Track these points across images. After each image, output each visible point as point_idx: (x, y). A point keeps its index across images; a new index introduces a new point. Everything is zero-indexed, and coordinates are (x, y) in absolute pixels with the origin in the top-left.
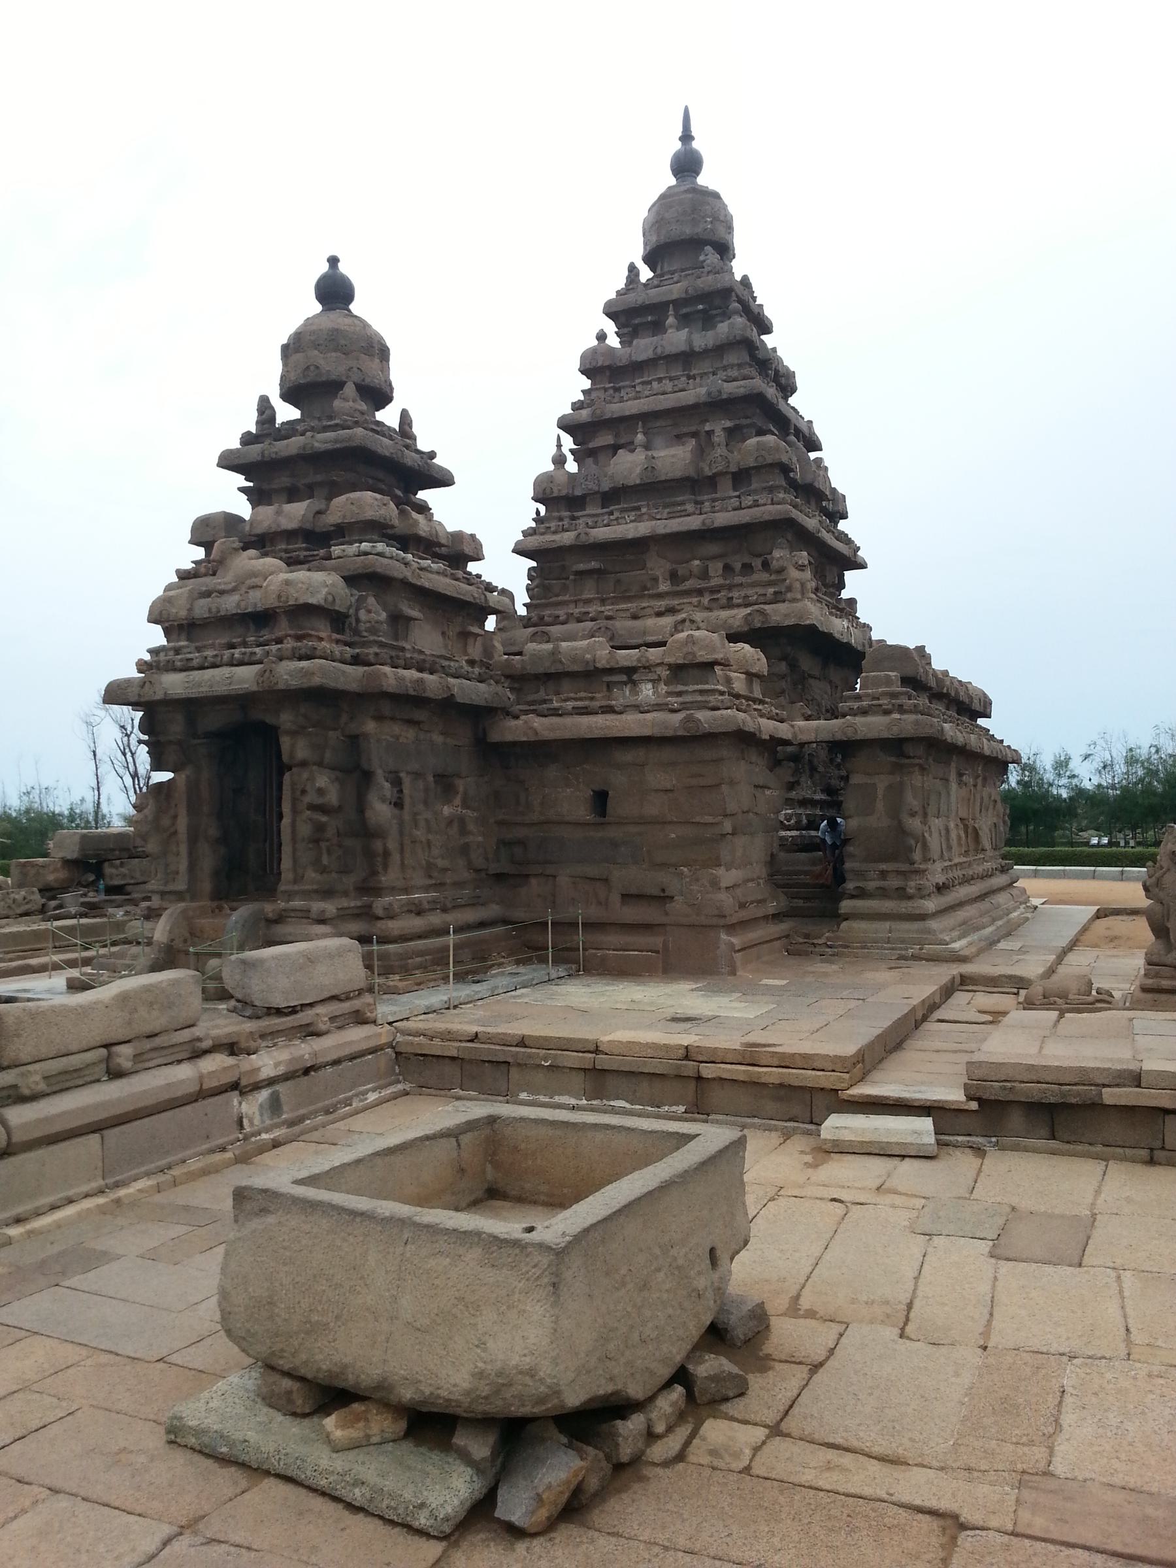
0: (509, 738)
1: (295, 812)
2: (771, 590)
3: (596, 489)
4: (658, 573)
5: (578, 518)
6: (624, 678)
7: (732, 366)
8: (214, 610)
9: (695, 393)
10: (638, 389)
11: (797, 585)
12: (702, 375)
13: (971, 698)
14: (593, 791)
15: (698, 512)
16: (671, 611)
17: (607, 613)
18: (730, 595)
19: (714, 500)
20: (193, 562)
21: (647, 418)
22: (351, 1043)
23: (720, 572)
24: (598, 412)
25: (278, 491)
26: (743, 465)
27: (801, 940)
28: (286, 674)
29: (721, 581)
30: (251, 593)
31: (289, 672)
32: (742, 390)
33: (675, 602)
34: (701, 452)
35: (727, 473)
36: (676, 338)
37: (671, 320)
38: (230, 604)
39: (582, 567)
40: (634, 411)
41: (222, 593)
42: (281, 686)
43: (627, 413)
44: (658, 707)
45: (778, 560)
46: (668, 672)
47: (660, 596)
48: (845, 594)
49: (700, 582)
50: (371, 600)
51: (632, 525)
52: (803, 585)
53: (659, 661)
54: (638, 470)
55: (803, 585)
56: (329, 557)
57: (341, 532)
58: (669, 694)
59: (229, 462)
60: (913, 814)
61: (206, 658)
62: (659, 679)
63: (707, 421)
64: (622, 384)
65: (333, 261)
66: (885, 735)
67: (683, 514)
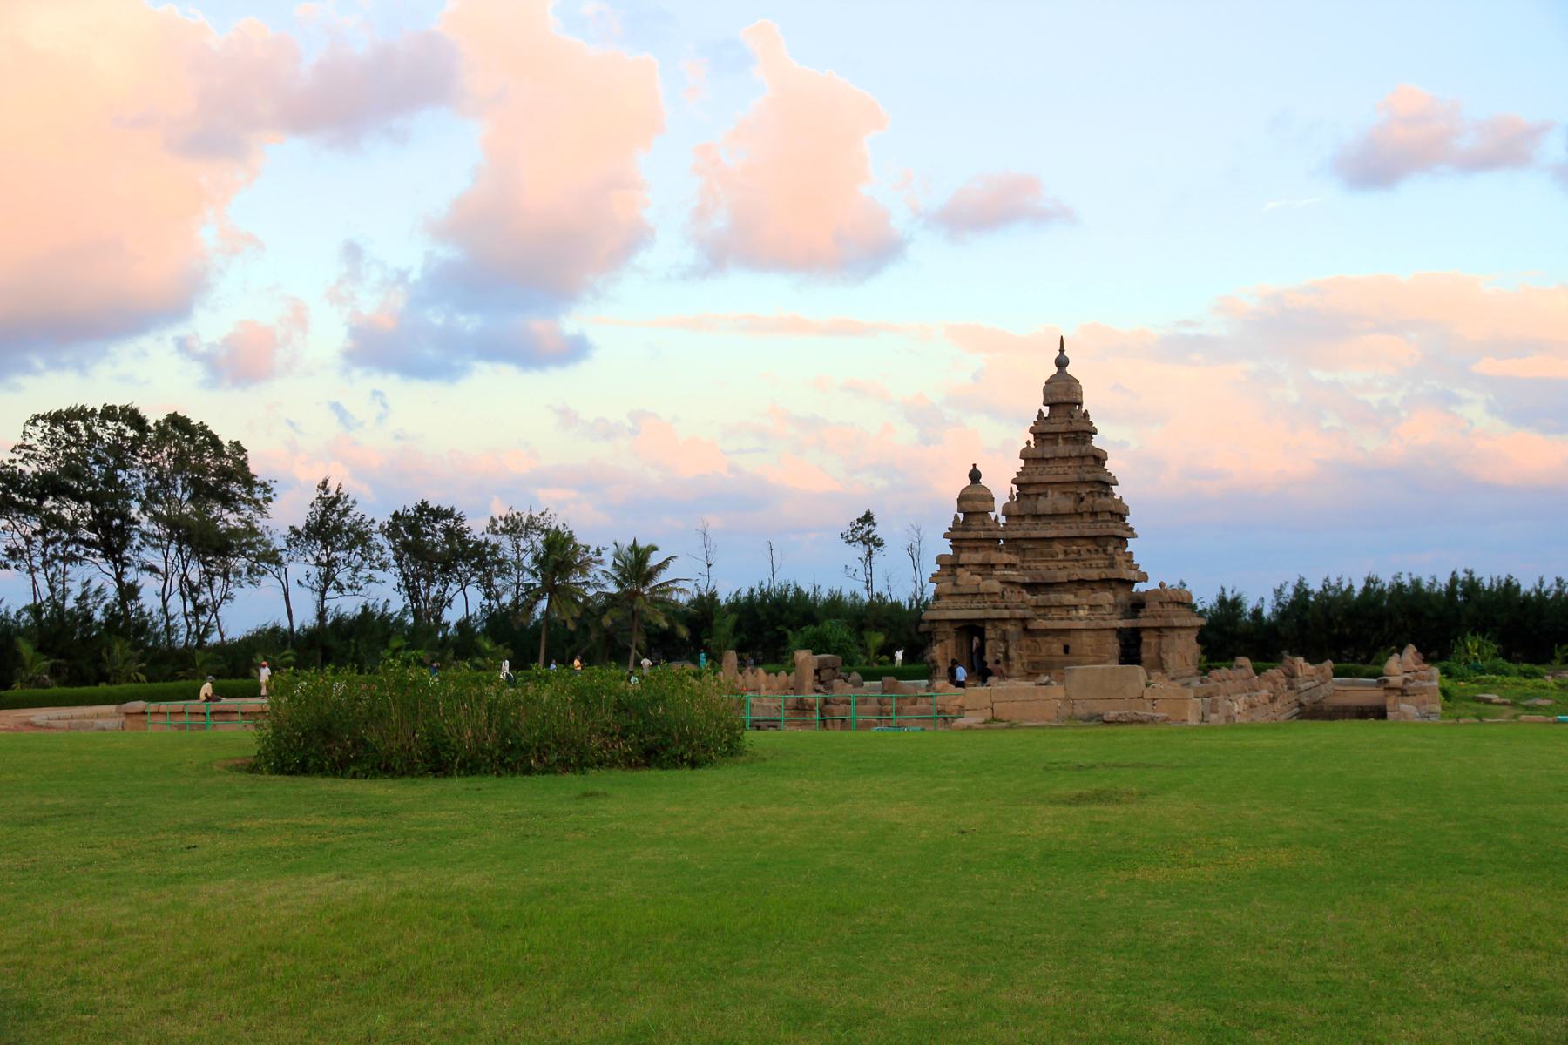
2: (1107, 562)
9: (1072, 477)
10: (1048, 469)
13: (1183, 598)
16: (1065, 567)
25: (965, 547)
31: (994, 614)
32: (1093, 479)
37: (1060, 441)
40: (1047, 481)
44: (1086, 619)
47: (1060, 561)
48: (1128, 550)
59: (946, 536)
60: (1164, 652)
65: (974, 465)
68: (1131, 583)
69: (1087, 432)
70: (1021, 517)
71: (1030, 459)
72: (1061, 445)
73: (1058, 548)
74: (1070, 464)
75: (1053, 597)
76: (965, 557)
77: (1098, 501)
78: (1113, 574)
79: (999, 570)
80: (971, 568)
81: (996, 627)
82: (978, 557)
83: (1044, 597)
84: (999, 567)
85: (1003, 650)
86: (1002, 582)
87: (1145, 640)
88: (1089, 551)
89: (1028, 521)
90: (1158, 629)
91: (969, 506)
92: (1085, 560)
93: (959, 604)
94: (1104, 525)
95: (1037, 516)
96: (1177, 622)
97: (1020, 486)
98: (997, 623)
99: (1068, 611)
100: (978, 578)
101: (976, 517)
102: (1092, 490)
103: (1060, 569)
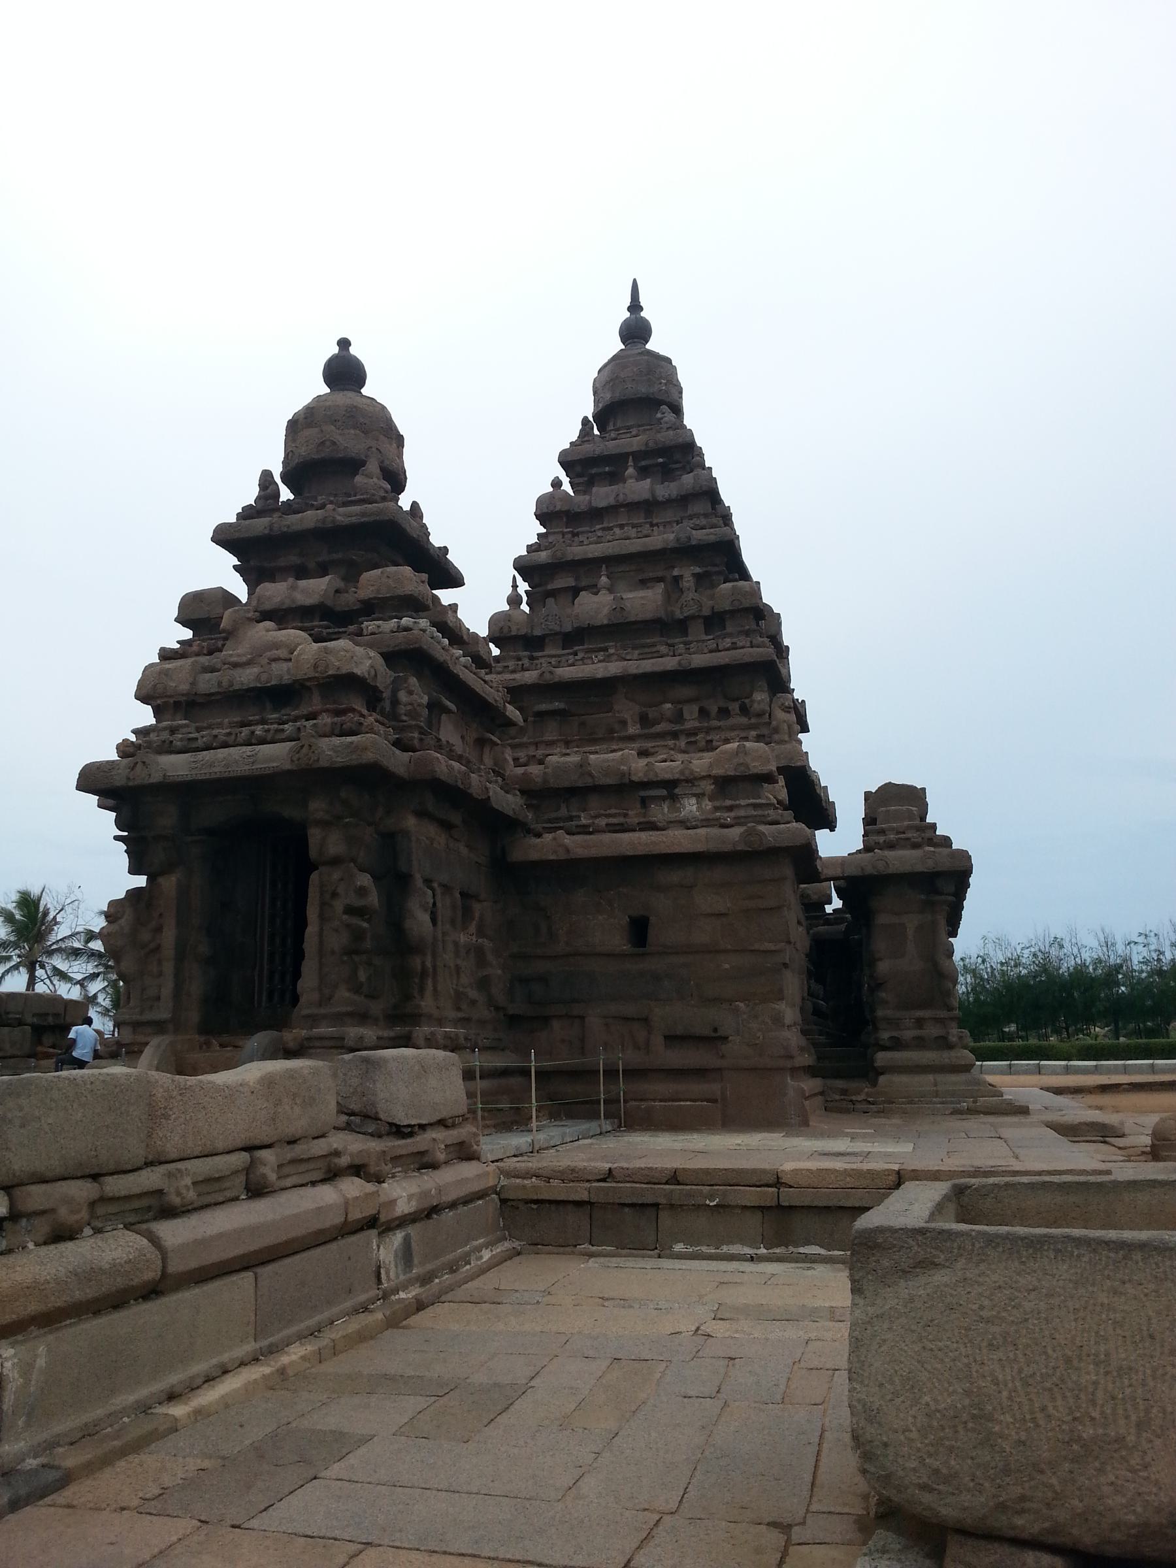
0: (534, 856)
1: (322, 918)
3: (557, 629)
4: (627, 716)
5: (537, 658)
6: (664, 792)
7: (697, 516)
8: (225, 684)
12: (665, 524)
14: (629, 917)
15: (672, 653)
18: (709, 738)
20: (178, 642)
21: (610, 561)
22: (465, 1180)
23: (696, 714)
24: (559, 554)
26: (717, 609)
27: (837, 1097)
28: (329, 750)
29: (697, 724)
30: (274, 665)
32: (712, 538)
33: (649, 745)
34: (668, 596)
35: (699, 617)
36: (637, 488)
37: (631, 471)
38: (246, 677)
39: (543, 707)
40: (596, 554)
41: (235, 665)
42: (324, 763)
43: (590, 556)
44: (707, 823)
45: (759, 702)
46: (713, 787)
47: (631, 738)
49: (673, 726)
50: (413, 680)
51: (600, 665)
52: (789, 727)
53: (704, 774)
54: (606, 611)
55: (789, 727)
56: (360, 634)
57: (370, 608)
58: (716, 809)
61: (216, 736)
62: (703, 794)
63: (673, 567)
64: (580, 529)
65: (344, 344)
66: (920, 868)
67: (655, 655)
74: (655, 521)
87: (882, 919)
94: (742, 641)
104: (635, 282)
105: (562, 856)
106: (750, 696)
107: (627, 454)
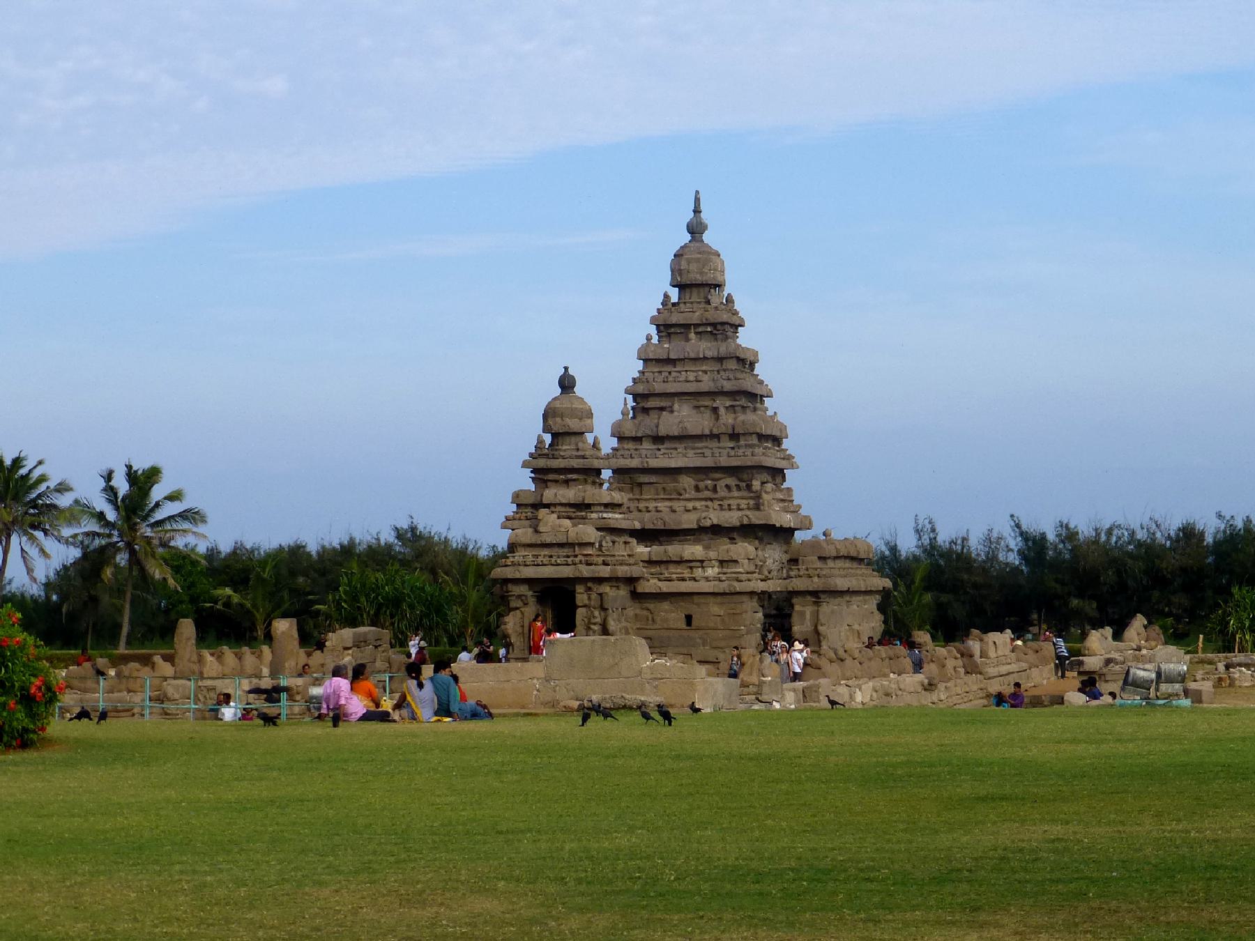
6: (699, 564)
9: (706, 384)
10: (674, 374)
11: (766, 502)
17: (658, 509)
19: (719, 448)
31: (586, 571)
32: (735, 388)
33: (698, 504)
37: (692, 335)
40: (673, 391)
43: (668, 391)
47: (689, 500)
48: (785, 485)
52: (768, 502)
59: (525, 465)
60: (822, 625)
65: (566, 369)
68: (790, 532)
69: (727, 323)
70: (637, 439)
71: (651, 360)
72: (693, 341)
73: (687, 481)
74: (704, 368)
75: (674, 549)
76: (550, 495)
77: (741, 417)
78: (759, 519)
79: (596, 512)
80: (559, 509)
81: (590, 589)
82: (569, 494)
83: (662, 548)
84: (598, 508)
85: (598, 620)
86: (598, 529)
87: (797, 608)
88: (727, 486)
89: (647, 445)
90: (815, 594)
91: (557, 424)
92: (722, 499)
93: (540, 559)
94: (749, 452)
95: (658, 439)
96: (842, 584)
97: (636, 397)
98: (590, 584)
99: (691, 568)
100: (567, 522)
101: (567, 439)
102: (734, 403)
103: (689, 511)
104: (697, 192)
105: (659, 591)
106: (751, 481)
107: (691, 325)
